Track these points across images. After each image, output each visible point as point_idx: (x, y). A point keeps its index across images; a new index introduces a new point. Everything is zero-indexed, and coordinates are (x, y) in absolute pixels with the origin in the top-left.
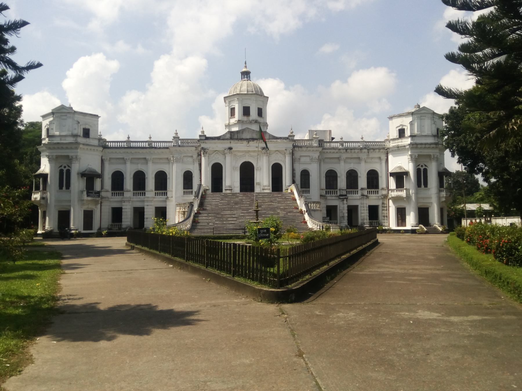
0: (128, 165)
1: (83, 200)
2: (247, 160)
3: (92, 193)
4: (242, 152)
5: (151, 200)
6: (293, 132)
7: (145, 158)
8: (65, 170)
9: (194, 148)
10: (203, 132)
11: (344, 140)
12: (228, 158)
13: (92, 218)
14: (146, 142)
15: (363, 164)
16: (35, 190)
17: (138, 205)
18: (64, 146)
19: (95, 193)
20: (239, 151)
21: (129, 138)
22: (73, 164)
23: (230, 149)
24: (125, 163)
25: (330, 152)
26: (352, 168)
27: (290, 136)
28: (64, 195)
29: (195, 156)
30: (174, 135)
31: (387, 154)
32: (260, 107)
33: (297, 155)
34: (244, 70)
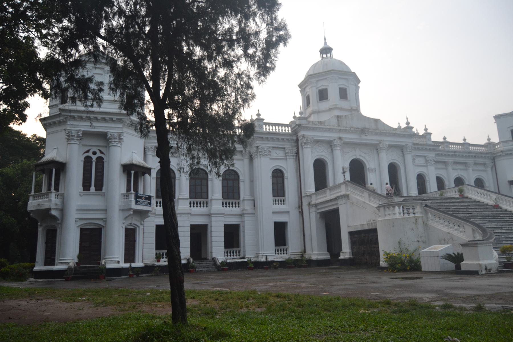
1: (130, 209)
2: (358, 157)
3: (141, 198)
5: (218, 214)
6: (408, 123)
8: (94, 158)
12: (338, 153)
13: (135, 241)
15: (470, 171)
16: (35, 192)
17: (199, 221)
18: (99, 116)
19: (146, 199)
22: (112, 149)
23: (340, 138)
28: (93, 201)
31: (493, 159)
34: (326, 46)
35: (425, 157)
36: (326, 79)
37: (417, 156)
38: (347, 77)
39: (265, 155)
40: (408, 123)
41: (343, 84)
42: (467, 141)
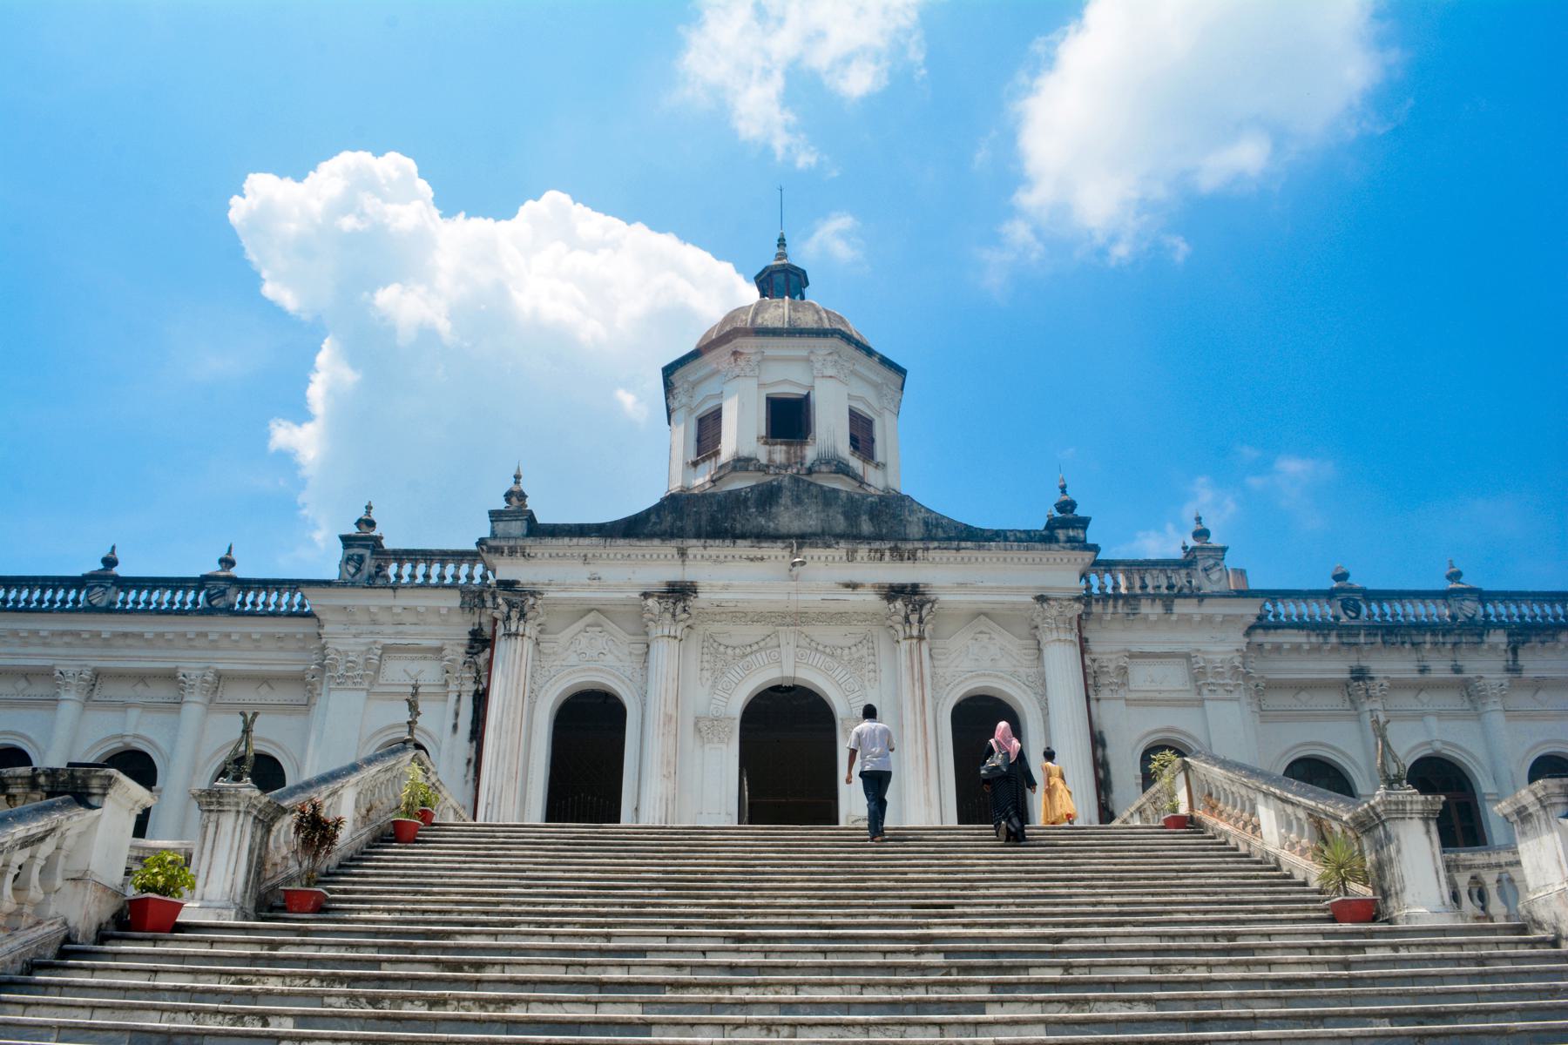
0: (69, 708)
4: (760, 617)
6: (1066, 506)
7: (171, 677)
9: (454, 599)
10: (516, 496)
11: (1360, 579)
12: (664, 654)
14: (201, 583)
15: (1496, 718)
20: (740, 615)
21: (110, 562)
24: (54, 701)
25: (1297, 648)
26: (1438, 746)
27: (1052, 525)
29: (457, 652)
30: (353, 530)
32: (861, 408)
33: (1110, 641)
35: (1187, 657)
36: (715, 373)
37: (1132, 656)
38: (804, 353)
39: (342, 681)
40: (1066, 506)
41: (785, 381)
42: (1468, 581)
